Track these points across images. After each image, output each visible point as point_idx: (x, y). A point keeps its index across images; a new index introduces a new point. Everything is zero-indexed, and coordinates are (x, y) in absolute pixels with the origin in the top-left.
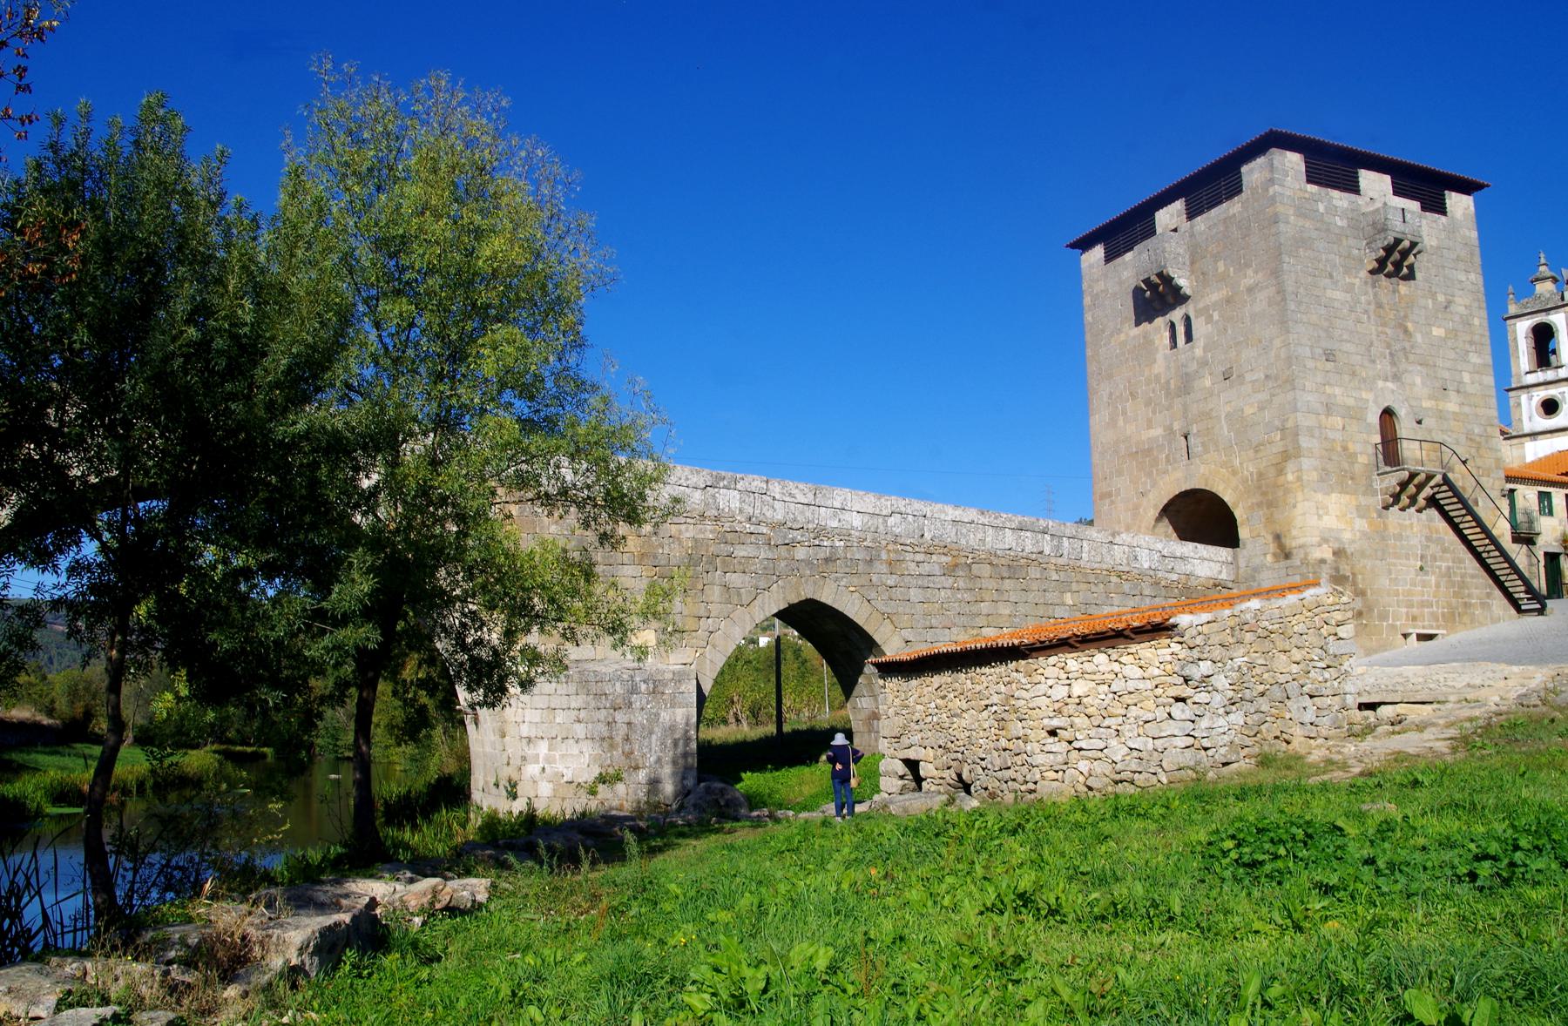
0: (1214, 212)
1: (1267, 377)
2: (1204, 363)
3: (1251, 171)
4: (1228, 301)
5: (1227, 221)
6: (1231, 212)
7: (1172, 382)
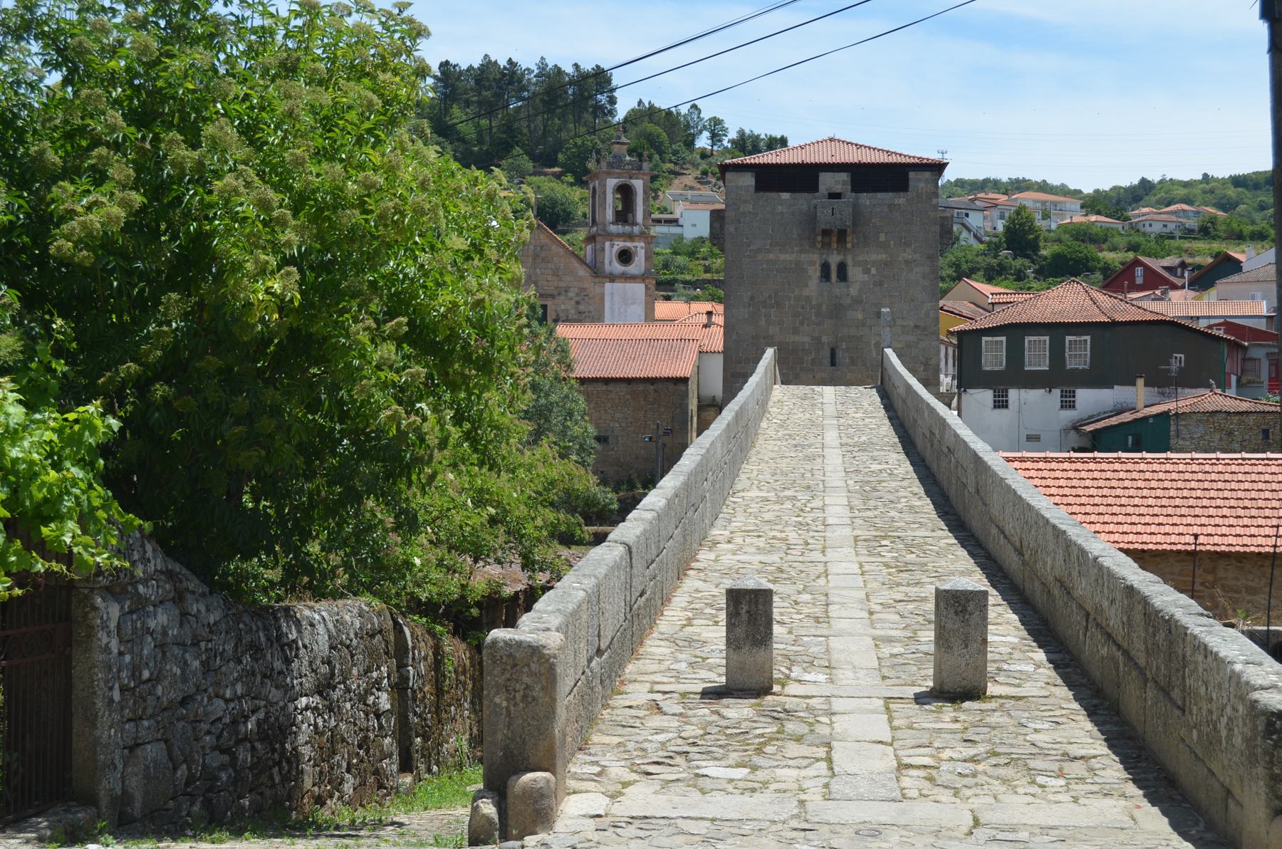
0: (880, 195)
1: (916, 326)
2: (858, 301)
3: (919, 180)
4: (886, 264)
5: (892, 207)
6: (896, 201)
7: (824, 307)
